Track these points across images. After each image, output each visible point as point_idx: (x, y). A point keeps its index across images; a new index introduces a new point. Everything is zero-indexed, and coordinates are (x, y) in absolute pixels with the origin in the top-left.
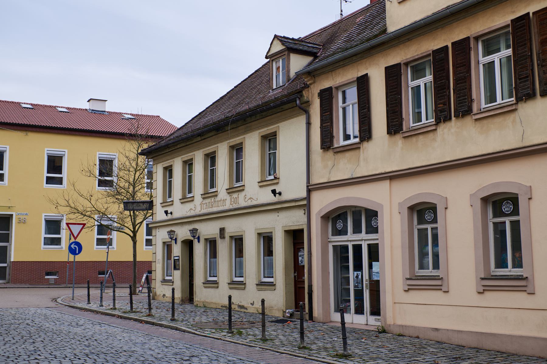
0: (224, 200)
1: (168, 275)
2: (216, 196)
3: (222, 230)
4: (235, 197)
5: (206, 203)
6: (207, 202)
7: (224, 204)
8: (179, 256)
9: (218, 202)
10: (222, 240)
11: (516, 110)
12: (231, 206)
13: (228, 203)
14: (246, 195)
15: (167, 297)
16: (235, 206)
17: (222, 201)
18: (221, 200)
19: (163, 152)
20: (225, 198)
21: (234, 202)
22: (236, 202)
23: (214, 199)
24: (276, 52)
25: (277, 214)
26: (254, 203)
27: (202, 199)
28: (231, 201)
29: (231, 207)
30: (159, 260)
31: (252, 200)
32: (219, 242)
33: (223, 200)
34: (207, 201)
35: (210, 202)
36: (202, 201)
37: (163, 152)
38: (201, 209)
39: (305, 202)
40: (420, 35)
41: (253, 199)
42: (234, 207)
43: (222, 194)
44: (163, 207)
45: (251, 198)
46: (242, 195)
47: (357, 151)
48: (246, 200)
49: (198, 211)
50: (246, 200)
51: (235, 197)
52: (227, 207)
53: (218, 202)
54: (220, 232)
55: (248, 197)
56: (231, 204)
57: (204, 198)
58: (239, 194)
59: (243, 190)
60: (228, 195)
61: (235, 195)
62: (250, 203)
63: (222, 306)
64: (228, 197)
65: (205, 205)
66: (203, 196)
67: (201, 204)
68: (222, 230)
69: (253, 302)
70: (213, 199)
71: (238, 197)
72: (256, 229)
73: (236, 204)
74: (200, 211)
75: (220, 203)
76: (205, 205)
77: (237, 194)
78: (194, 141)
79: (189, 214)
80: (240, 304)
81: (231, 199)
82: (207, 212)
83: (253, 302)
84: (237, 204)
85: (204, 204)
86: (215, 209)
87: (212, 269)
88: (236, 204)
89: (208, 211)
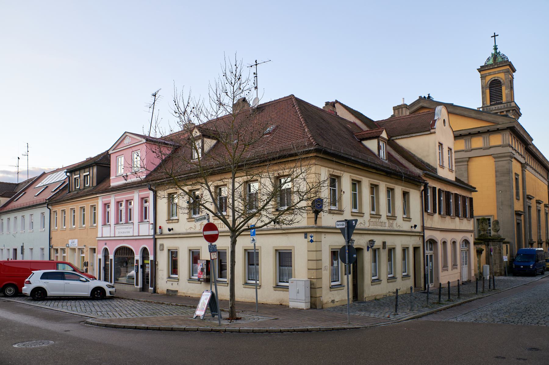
0: (385, 223)
1: (337, 280)
2: (380, 218)
3: (384, 243)
5: (373, 221)
6: (373, 221)
7: (385, 226)
10: (384, 250)
11: (455, 218)
12: (389, 228)
13: (387, 225)
15: (337, 302)
16: (391, 229)
18: (383, 222)
19: (354, 165)
20: (385, 221)
23: (378, 220)
24: (382, 137)
25: (411, 238)
26: (401, 229)
27: (370, 218)
28: (389, 225)
29: (389, 228)
30: (326, 266)
32: (381, 249)
36: (370, 219)
38: (370, 226)
39: (422, 234)
40: (444, 183)
42: (391, 229)
43: (384, 218)
44: (352, 215)
45: (399, 226)
46: (395, 222)
48: (397, 226)
49: (367, 226)
50: (397, 226)
52: (386, 228)
55: (398, 225)
57: (371, 217)
60: (387, 220)
61: (391, 221)
63: (384, 296)
64: (386, 221)
67: (369, 221)
68: (384, 243)
69: (400, 288)
70: (377, 219)
72: (401, 245)
74: (368, 226)
75: (382, 223)
76: (372, 223)
77: (392, 221)
80: (393, 291)
81: (389, 223)
82: (373, 228)
83: (400, 288)
85: (371, 222)
86: (379, 228)
87: (376, 271)
88: (392, 227)
89: (374, 227)
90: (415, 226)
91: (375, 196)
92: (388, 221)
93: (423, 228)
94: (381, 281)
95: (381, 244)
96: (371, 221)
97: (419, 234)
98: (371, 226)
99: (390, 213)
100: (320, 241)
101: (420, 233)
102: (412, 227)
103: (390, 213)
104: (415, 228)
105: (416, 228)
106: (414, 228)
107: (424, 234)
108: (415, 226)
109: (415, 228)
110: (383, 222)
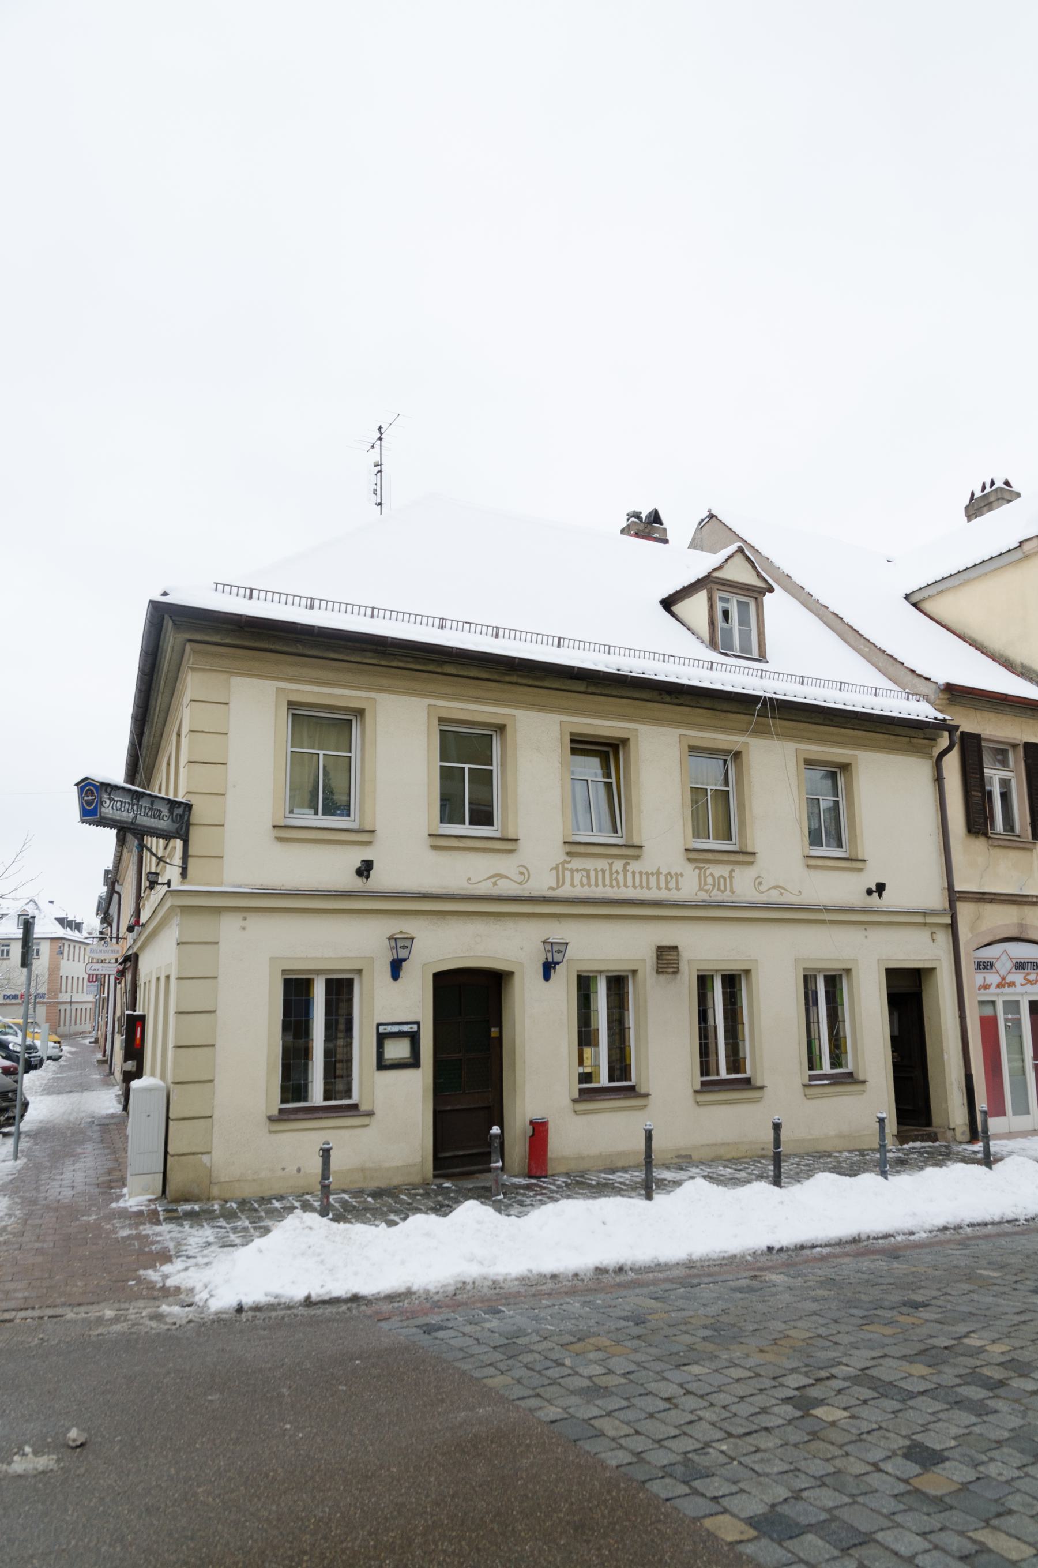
4: (717, 875)
8: (418, 1023)
9: (644, 877)
14: (759, 877)
16: (717, 896)
17: (662, 878)
18: (658, 873)
21: (714, 886)
22: (722, 888)
29: (703, 896)
31: (782, 891)
33: (669, 873)
34: (577, 863)
35: (603, 871)
36: (565, 862)
37: (332, 655)
41: (785, 889)
47: (1028, 854)
48: (763, 888)
49: (542, 883)
51: (717, 875)
53: (644, 877)
54: (658, 956)
56: (701, 889)
58: (732, 871)
59: (752, 863)
62: (774, 897)
65: (577, 877)
66: (568, 848)
67: (556, 868)
70: (618, 865)
71: (731, 877)
73: (723, 892)
77: (728, 868)
78: (546, 684)
79: (485, 888)
84: (728, 892)
86: (630, 893)
90: (881, 888)
91: (614, 780)
92: (700, 868)
93: (954, 897)
94: (646, 1095)
95: (650, 956)
96: (572, 871)
97: (919, 919)
98: (604, 885)
99: (730, 839)
100: (183, 943)
101: (933, 913)
102: (869, 892)
103: (730, 839)
104: (880, 896)
105: (884, 893)
106: (876, 895)
107: (954, 917)
108: (881, 888)
109: (880, 896)
110: (658, 873)
